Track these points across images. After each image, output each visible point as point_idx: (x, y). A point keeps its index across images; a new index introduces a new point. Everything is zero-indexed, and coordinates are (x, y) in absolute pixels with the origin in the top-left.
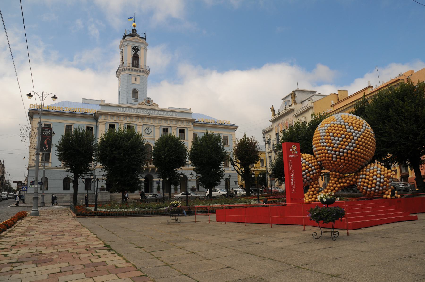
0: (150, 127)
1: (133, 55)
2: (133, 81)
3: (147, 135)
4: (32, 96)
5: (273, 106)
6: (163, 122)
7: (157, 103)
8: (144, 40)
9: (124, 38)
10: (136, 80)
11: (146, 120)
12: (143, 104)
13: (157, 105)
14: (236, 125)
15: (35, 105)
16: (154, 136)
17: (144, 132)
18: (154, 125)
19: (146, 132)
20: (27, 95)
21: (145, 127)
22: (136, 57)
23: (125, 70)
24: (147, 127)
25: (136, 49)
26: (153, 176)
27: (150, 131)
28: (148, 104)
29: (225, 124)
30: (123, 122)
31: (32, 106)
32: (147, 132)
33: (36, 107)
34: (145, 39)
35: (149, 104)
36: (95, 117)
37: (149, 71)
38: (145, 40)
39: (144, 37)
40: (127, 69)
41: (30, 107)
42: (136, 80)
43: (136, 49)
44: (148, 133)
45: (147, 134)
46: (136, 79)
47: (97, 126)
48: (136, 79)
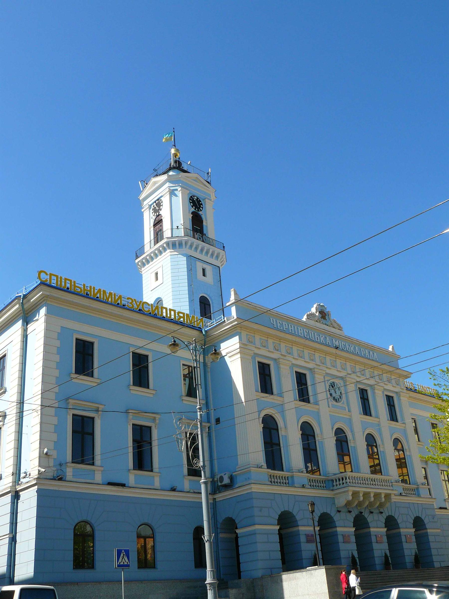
3: (334, 403)
15: (51, 275)
26: (369, 520)
40: (186, 243)
41: (39, 277)
46: (204, 270)
48: (204, 270)
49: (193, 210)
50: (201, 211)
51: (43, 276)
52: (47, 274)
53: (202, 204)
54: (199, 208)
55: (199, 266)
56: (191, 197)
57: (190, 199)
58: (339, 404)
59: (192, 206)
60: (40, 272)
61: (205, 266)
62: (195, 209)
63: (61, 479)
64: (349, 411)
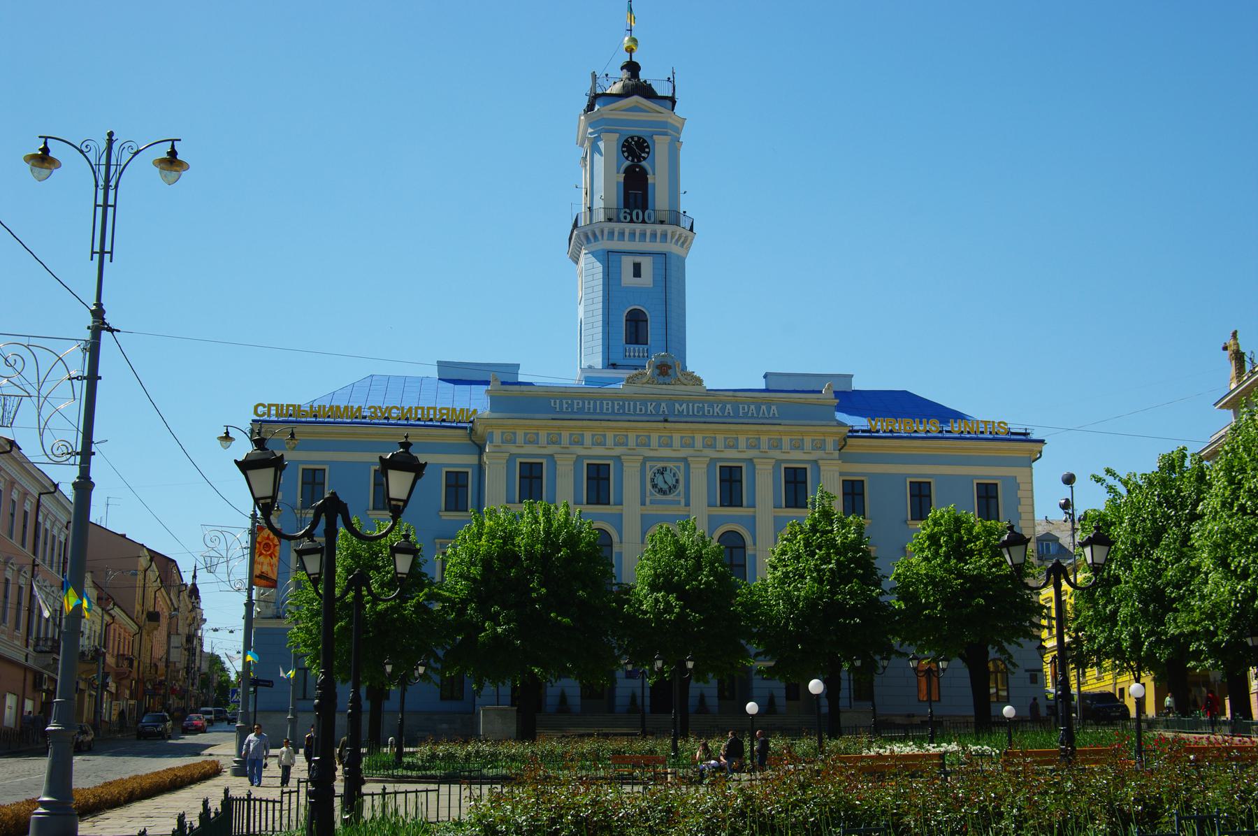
1: (627, 171)
2: (627, 278)
3: (659, 497)
4: (232, 439)
5: (1234, 335)
7: (697, 374)
8: (669, 104)
9: (590, 107)
10: (637, 271)
13: (699, 381)
14: (1034, 436)
15: (270, 405)
17: (649, 486)
19: (655, 486)
20: (221, 438)
23: (595, 235)
24: (660, 465)
25: (635, 149)
27: (671, 481)
29: (987, 435)
31: (261, 409)
32: (661, 484)
33: (273, 412)
34: (672, 100)
36: (472, 435)
37: (691, 229)
38: (674, 103)
41: (256, 412)
42: (637, 271)
43: (635, 149)
44: (665, 487)
45: (662, 491)
47: (480, 468)
49: (628, 163)
50: (644, 159)
51: (261, 409)
52: (264, 406)
53: (648, 147)
54: (640, 158)
55: (627, 263)
56: (626, 141)
57: (623, 146)
58: (670, 497)
60: (256, 407)
61: (638, 259)
63: (279, 617)
64: (687, 504)
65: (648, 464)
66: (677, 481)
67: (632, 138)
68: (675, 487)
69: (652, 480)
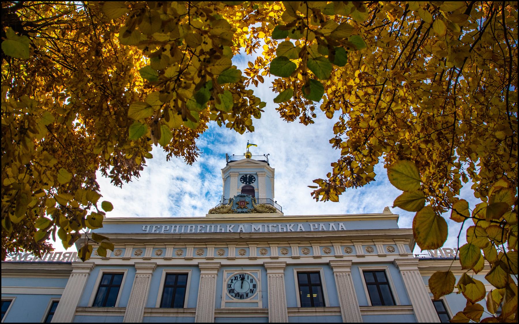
0: (247, 271)
1: (243, 188)
3: (236, 300)
6: (296, 250)
11: (232, 251)
12: (225, 210)
16: (265, 298)
17: (225, 291)
18: (262, 266)
19: (231, 291)
21: (227, 275)
22: (248, 191)
24: (237, 272)
25: (248, 180)
27: (247, 286)
28: (240, 210)
30: (152, 261)
32: (238, 289)
35: (245, 210)
39: (266, 160)
43: (248, 180)
44: (241, 291)
45: (239, 296)
53: (254, 178)
56: (243, 176)
57: (241, 178)
59: (243, 183)
62: (246, 184)
65: (225, 274)
66: (255, 286)
67: (246, 175)
68: (252, 291)
69: (229, 286)
